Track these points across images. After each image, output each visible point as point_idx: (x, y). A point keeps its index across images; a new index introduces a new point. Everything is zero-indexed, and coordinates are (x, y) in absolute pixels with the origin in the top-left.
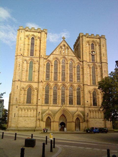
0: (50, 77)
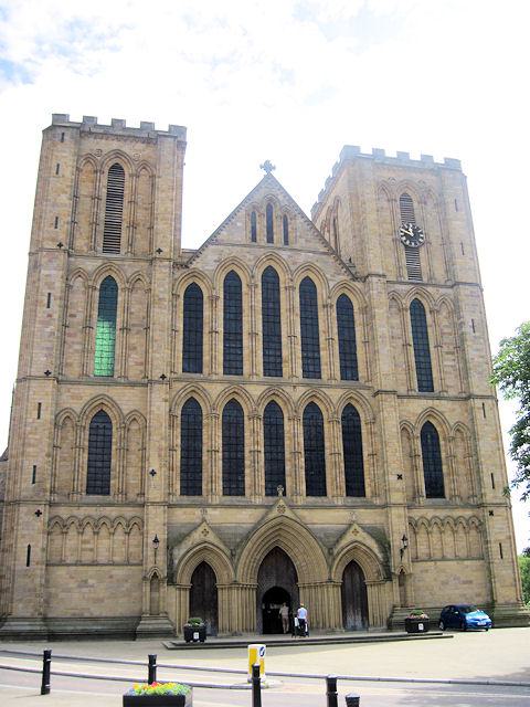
0: (206, 358)
